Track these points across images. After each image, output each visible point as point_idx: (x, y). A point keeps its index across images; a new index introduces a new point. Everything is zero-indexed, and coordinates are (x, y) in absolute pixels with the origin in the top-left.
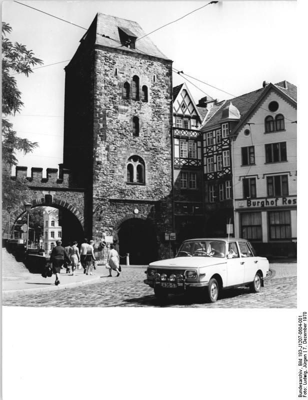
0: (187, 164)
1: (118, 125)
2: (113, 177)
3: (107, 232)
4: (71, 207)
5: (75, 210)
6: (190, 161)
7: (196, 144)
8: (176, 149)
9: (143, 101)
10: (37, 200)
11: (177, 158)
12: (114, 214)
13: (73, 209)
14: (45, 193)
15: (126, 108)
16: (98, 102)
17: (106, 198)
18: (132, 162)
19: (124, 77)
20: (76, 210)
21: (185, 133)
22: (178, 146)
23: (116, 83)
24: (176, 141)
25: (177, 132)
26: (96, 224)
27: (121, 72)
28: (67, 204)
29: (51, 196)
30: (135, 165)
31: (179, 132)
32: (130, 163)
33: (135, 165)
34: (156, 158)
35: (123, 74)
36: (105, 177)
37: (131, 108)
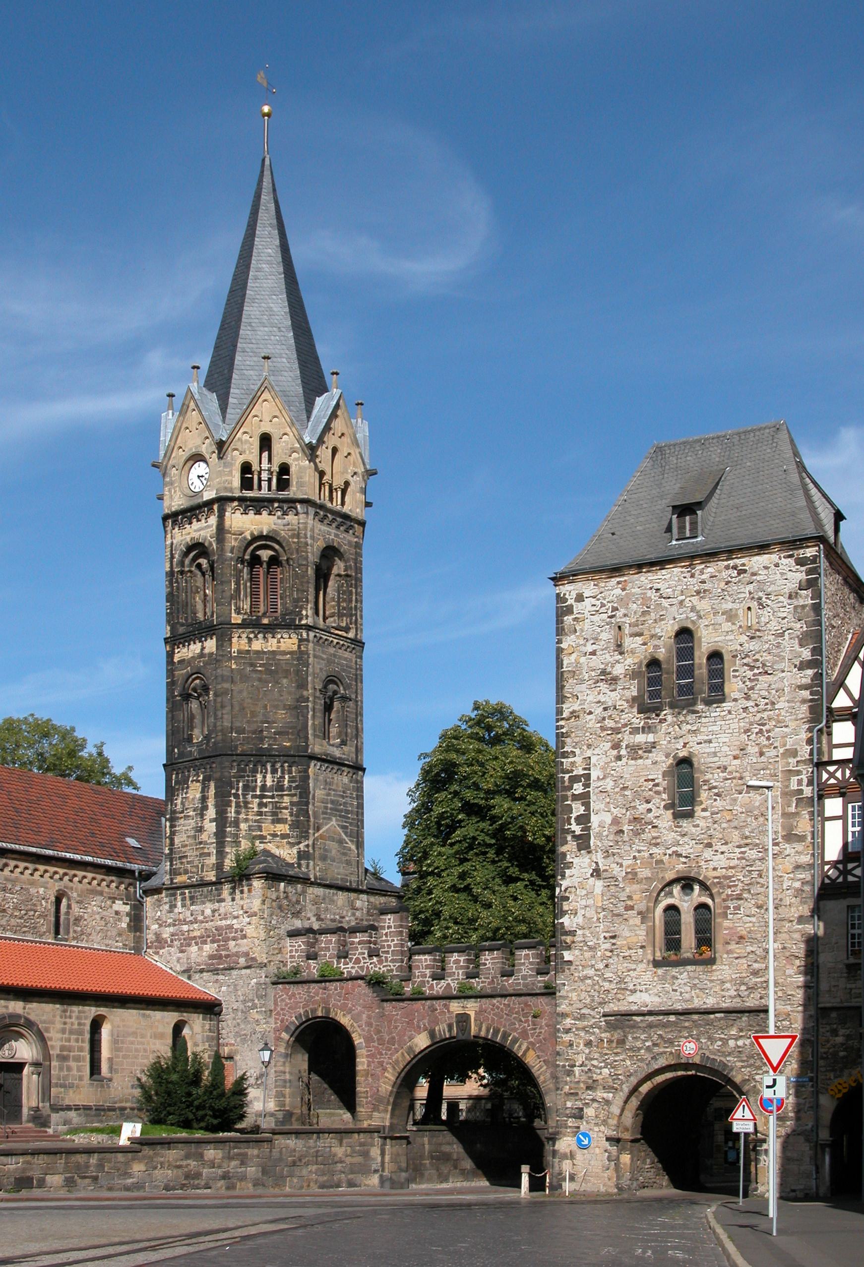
1: (624, 796)
2: (612, 951)
3: (595, 1105)
4: (515, 1041)
5: (524, 1047)
9: (708, 703)
10: (437, 1028)
12: (616, 1054)
13: (520, 1046)
14: (456, 1007)
15: (651, 738)
16: (568, 740)
17: (592, 1013)
18: (677, 896)
19: (644, 644)
20: (528, 1049)
22: (840, 823)
23: (619, 670)
25: (832, 775)
26: (566, 1083)
27: (636, 629)
28: (505, 1035)
29: (468, 1016)
30: (686, 903)
32: (670, 901)
33: (686, 903)
34: (755, 874)
35: (640, 634)
36: (588, 955)
37: (673, 734)
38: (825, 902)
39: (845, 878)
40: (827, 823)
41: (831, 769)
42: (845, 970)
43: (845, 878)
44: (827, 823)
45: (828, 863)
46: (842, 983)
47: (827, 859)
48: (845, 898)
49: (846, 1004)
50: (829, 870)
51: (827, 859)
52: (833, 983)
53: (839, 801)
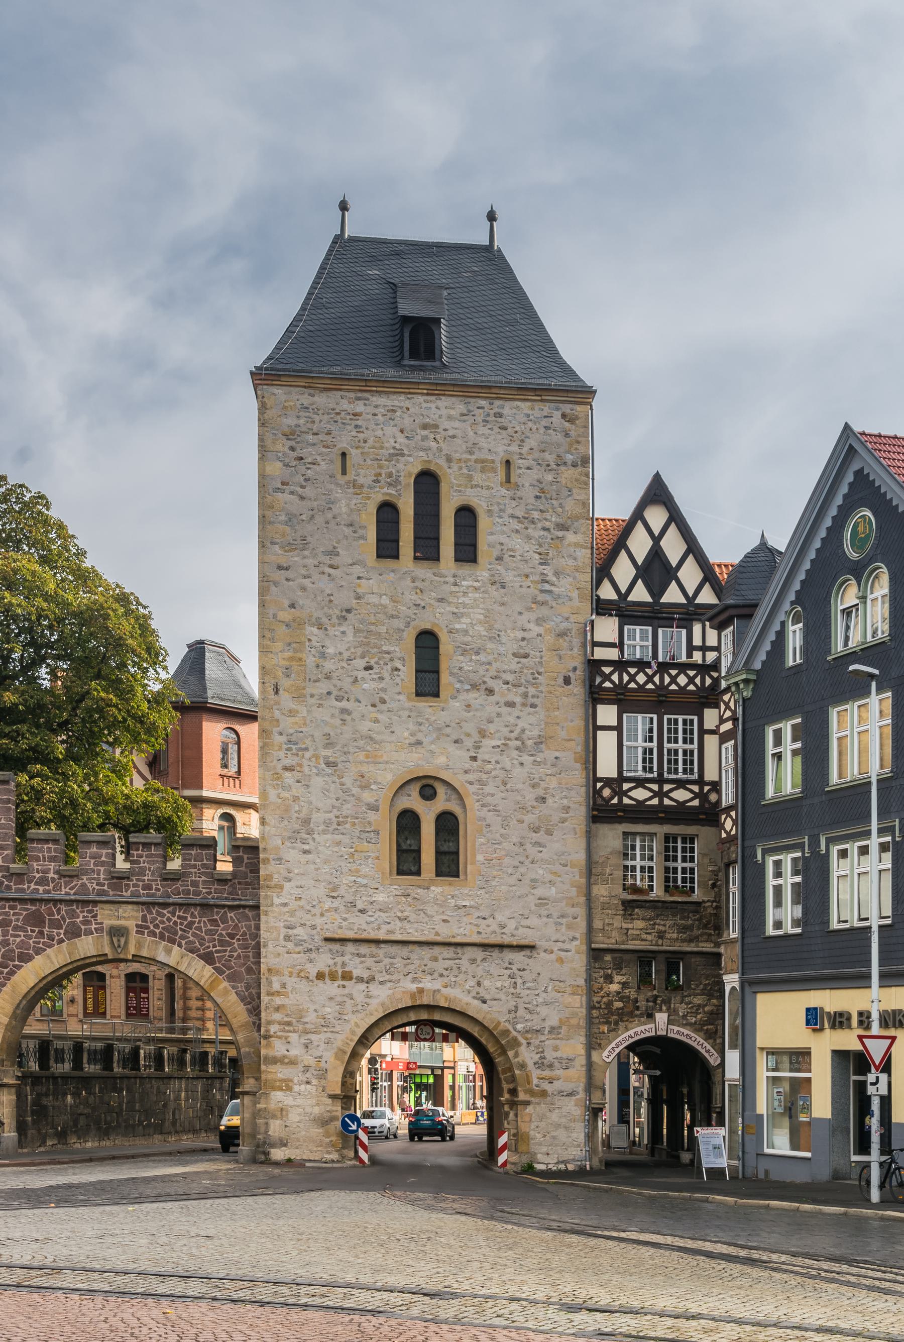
0: (655, 801)
6: (666, 787)
7: (696, 718)
8: (607, 742)
11: (608, 782)
21: (641, 678)
24: (607, 714)
31: (615, 677)
38: (598, 825)
39: (620, 800)
40: (599, 733)
41: (607, 670)
42: (621, 908)
43: (620, 800)
44: (599, 733)
45: (601, 779)
46: (618, 922)
47: (599, 775)
48: (620, 823)
49: (623, 947)
50: (602, 788)
51: (599, 775)
52: (607, 921)
53: (613, 709)
